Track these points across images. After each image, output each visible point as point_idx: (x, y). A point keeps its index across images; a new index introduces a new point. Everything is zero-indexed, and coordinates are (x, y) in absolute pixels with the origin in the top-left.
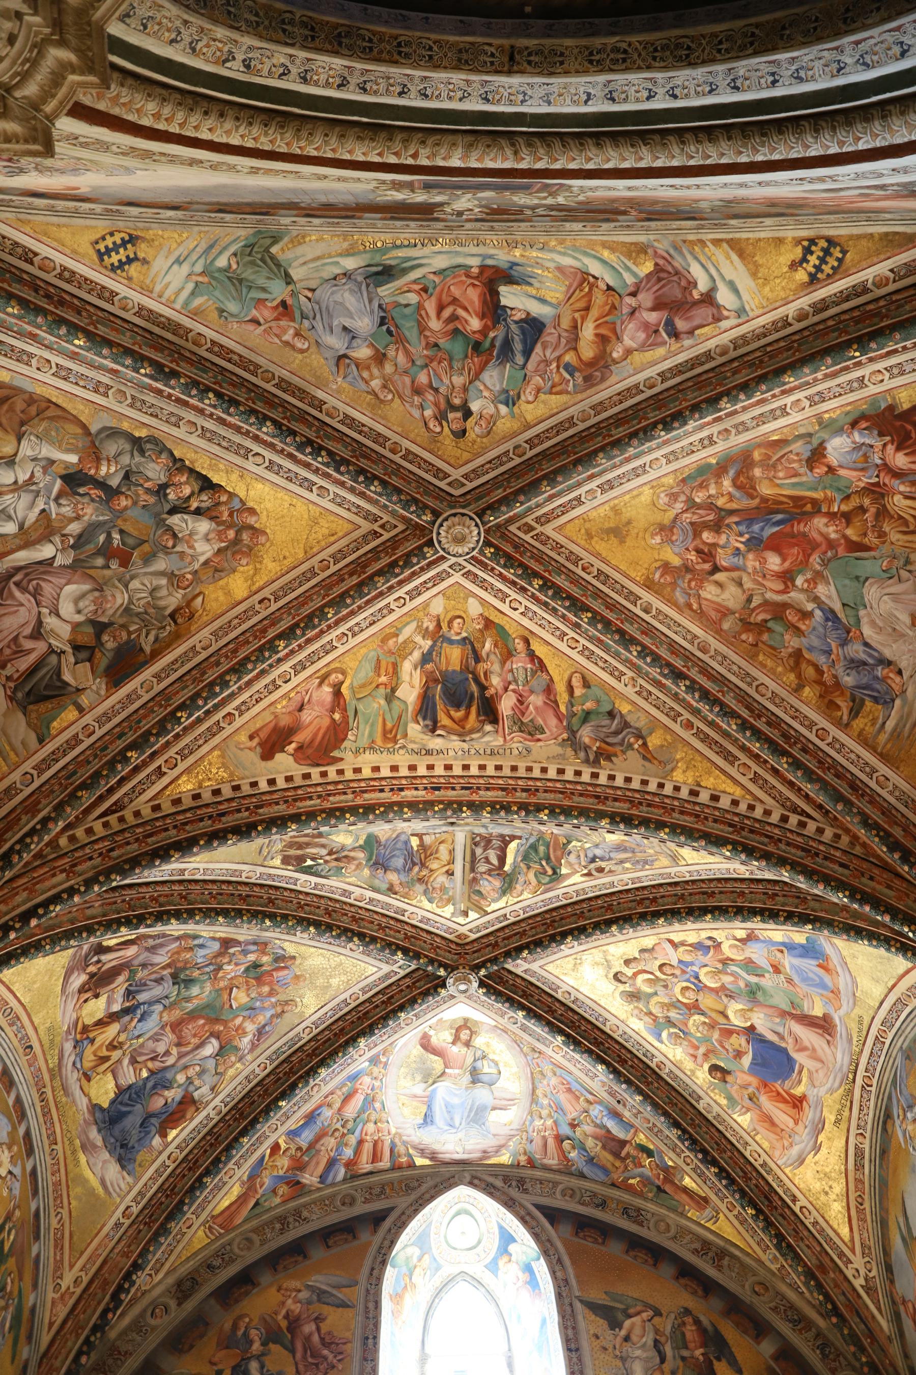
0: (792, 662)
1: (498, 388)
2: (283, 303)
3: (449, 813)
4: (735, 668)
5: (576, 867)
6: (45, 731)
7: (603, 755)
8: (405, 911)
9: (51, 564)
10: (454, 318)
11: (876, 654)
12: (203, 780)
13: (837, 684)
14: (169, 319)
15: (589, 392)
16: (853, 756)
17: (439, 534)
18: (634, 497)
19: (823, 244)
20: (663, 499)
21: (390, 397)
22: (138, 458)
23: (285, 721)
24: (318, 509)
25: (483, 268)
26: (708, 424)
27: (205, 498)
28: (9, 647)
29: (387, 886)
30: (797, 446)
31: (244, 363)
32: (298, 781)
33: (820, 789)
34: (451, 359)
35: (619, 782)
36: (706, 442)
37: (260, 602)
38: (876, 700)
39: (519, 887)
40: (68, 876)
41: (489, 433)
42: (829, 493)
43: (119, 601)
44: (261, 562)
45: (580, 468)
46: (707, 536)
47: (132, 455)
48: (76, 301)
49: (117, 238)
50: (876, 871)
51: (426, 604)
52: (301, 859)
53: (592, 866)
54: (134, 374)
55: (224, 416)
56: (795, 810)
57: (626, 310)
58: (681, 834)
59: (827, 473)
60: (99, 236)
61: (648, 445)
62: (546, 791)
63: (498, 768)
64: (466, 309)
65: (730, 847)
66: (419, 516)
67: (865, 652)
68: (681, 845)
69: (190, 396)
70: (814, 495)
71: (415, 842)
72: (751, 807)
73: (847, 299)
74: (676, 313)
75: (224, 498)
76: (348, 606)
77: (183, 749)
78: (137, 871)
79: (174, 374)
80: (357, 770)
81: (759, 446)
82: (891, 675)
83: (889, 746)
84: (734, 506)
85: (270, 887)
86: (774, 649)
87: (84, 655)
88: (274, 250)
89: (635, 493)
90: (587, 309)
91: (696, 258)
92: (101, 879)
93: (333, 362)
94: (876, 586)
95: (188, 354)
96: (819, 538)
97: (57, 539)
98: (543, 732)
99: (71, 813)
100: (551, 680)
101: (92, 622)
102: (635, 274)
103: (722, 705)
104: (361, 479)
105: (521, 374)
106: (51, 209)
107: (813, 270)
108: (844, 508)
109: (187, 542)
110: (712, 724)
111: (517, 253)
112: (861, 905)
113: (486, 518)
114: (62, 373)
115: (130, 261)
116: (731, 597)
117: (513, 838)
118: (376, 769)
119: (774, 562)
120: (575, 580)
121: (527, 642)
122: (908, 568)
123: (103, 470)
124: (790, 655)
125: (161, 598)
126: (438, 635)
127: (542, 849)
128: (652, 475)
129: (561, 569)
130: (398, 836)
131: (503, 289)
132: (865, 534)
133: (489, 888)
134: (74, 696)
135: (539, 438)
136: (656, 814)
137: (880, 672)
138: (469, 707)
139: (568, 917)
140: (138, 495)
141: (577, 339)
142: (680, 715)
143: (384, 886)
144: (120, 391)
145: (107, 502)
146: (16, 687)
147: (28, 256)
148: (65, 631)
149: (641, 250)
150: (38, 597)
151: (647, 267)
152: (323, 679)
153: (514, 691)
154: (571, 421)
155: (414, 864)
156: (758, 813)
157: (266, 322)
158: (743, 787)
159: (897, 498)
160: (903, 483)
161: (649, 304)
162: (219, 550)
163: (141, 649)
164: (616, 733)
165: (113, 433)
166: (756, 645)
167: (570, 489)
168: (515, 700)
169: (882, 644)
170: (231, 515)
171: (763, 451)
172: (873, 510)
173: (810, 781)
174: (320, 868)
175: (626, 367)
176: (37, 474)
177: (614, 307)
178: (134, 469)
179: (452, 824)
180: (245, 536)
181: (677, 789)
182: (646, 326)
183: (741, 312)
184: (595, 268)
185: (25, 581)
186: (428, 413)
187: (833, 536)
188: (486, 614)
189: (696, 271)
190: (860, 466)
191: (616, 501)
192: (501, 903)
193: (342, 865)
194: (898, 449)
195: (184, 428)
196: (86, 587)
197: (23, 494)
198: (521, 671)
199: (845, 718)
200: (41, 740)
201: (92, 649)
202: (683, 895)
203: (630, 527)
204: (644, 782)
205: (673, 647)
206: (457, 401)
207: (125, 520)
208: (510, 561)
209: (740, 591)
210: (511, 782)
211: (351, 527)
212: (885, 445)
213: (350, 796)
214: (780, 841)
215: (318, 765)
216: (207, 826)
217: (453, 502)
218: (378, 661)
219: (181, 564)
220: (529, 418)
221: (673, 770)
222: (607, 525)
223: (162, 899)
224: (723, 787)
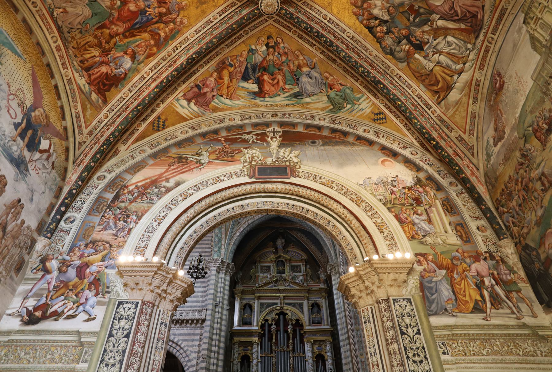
2: (331, 89)
9: (441, 17)
10: (273, 80)
15: (223, 58)
20: (185, 21)
21: (296, 52)
22: (393, 48)
25: (264, 97)
27: (372, 24)
30: (141, 58)
31: (347, 72)
34: (274, 65)
36: (175, 49)
41: (258, 38)
46: (164, 10)
49: (379, 122)
59: (127, 51)
64: (269, 83)
70: (126, 40)
73: (147, 116)
75: (365, 22)
81: (154, 54)
84: (156, 25)
88: (332, 107)
90: (228, 87)
94: (87, 14)
97: (434, 26)
102: (215, 102)
105: (248, 61)
108: (114, 40)
109: (384, 6)
113: (258, 11)
115: (377, 114)
122: (79, 30)
123: (407, 47)
131: (257, 90)
132: (102, 33)
135: (239, 38)
140: (398, 33)
141: (230, 76)
144: (392, 74)
154: (228, 46)
159: (98, 54)
160: (99, 61)
161: (208, 94)
165: (400, 60)
170: (364, 14)
171: (153, 52)
172: (104, 44)
176: (431, 55)
177: (219, 90)
178: (396, 44)
182: (207, 86)
184: (228, 101)
185: (454, 15)
186: (282, 45)
189: (195, 108)
190: (116, 60)
194: (107, 73)
195: (374, 54)
206: (271, 50)
207: (406, 24)
212: (112, 72)
220: (243, 45)
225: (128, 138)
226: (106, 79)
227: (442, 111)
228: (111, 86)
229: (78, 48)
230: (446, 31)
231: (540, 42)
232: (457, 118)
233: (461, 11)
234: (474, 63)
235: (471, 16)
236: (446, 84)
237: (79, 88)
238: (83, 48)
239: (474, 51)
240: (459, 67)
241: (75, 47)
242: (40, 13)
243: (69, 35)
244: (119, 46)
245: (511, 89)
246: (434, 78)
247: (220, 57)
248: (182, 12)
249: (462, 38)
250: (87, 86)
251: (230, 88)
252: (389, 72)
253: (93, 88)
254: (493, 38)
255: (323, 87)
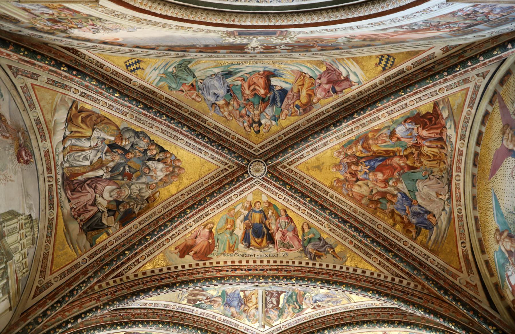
0: (390, 215)
1: (271, 115)
2: (192, 85)
3: (255, 280)
4: (368, 218)
5: (309, 305)
6: (93, 242)
7: (317, 256)
8: (239, 325)
9: (102, 178)
10: (254, 89)
11: (424, 209)
12: (156, 265)
13: (410, 223)
14: (150, 89)
15: (305, 115)
16: (419, 252)
17: (250, 168)
18: (324, 154)
19: (386, 57)
20: (336, 154)
21: (231, 118)
22: (137, 139)
23: (190, 242)
24: (204, 160)
25: (264, 71)
26: (350, 124)
28: (82, 208)
29: (231, 314)
30: (385, 131)
31: (178, 106)
32: (194, 267)
33: (407, 265)
34: (254, 105)
35: (324, 266)
36: (350, 131)
37: (181, 195)
38: (426, 228)
39: (285, 314)
40: (96, 302)
41: (268, 131)
42: (399, 148)
43: (127, 193)
44: (182, 180)
45: (303, 143)
46: (353, 167)
47: (135, 138)
48: (117, 82)
49: (133, 61)
50: (434, 300)
51: (246, 197)
52: (195, 301)
53: (315, 304)
54: (137, 108)
55: (169, 124)
56: (397, 275)
57: (317, 85)
58: (350, 287)
60: (127, 60)
61: (328, 133)
62: (294, 271)
63: (275, 262)
64: (259, 86)
65: (371, 292)
66: (242, 162)
67: (419, 209)
68: (351, 293)
69: (157, 116)
71: (242, 294)
72: (379, 275)
73: (397, 75)
74: (335, 85)
75: (169, 155)
76: (215, 197)
77: (148, 252)
78: (125, 301)
79: (151, 108)
80: (218, 263)
81: (371, 132)
82: (431, 217)
83: (433, 246)
84: (363, 155)
85: (182, 313)
86: (383, 210)
87: (111, 213)
88: (189, 66)
89: (325, 152)
90: (303, 85)
91: (341, 65)
92: (110, 303)
93: (210, 106)
94: (421, 183)
95: (157, 102)
96: (397, 166)
97: (104, 168)
98: (293, 247)
99: (101, 275)
100: (295, 226)
101: (116, 201)
102: (319, 72)
103: (364, 233)
104: (220, 148)
106: (111, 50)
107: (384, 66)
108: (405, 153)
109: (154, 172)
110: (360, 241)
111: (277, 66)
112: (429, 315)
113: (268, 163)
114: (111, 107)
115: (137, 69)
116: (364, 190)
117: (282, 292)
118: (226, 262)
119: (380, 176)
120: (303, 186)
121: (285, 211)
122: (433, 174)
123: (124, 143)
124: (390, 212)
125: (143, 193)
126: (250, 209)
127: (294, 297)
128: (331, 145)
129: (297, 182)
130: (235, 292)
131: (272, 79)
132: (414, 163)
133: (273, 315)
134: (106, 229)
135: (287, 133)
136: (340, 279)
137: (426, 216)
138: (263, 238)
139: (307, 328)
140: (136, 153)
141: (300, 96)
142: (347, 238)
143: (230, 314)
144: (131, 114)
145: (125, 155)
146: (84, 225)
147: (101, 66)
148: (105, 204)
149: (321, 63)
150: (96, 190)
151: (324, 69)
152: (205, 226)
153: (281, 231)
154: (299, 127)
155: (242, 304)
156: (382, 277)
157: (186, 91)
158: (375, 267)
159: (425, 148)
160: (427, 142)
161: (325, 82)
162: (166, 175)
163: (134, 212)
164: (322, 247)
165: (128, 130)
166: (376, 209)
167: (300, 151)
168: (281, 235)
169: (426, 205)
170: (171, 162)
171: (372, 133)
172: (416, 153)
173: (402, 262)
174: (203, 305)
175: (318, 105)
176: (99, 144)
177: (313, 83)
179: (257, 286)
180: (176, 170)
181: (348, 269)
183: (359, 83)
184: (305, 70)
186: (246, 124)
187: (402, 164)
188: (269, 201)
189: (341, 69)
190: (409, 137)
191: (318, 156)
192: (278, 322)
193: (212, 304)
194: (423, 129)
195: (154, 129)
196: (114, 187)
197: (93, 151)
198: (283, 223)
199: (414, 236)
200: (92, 246)
201: (115, 211)
202: (354, 316)
203: (324, 165)
204: (335, 267)
205: (343, 211)
206: (256, 120)
208: (277, 179)
209: (367, 188)
210: (280, 267)
211: (217, 167)
212: (418, 128)
213: (215, 273)
214: (392, 288)
215: (202, 260)
216: (156, 283)
217: (255, 157)
218: (227, 219)
219: (151, 180)
220: (284, 125)
221: (346, 261)
222: (315, 165)
223: (136, 316)
224: (367, 267)
225: (426, 59)
226: (426, 124)
227: (67, 96)
228: (424, 116)
229: (440, 160)
230: (93, 167)
231: (7, 221)
232: (48, 96)
233: (86, 189)
234: (56, 153)
235: (76, 190)
236: (74, 123)
237: (456, 128)
238: (436, 158)
239: (60, 163)
240: (68, 144)
241: (442, 163)
242: (459, 203)
243: (443, 175)
244: (402, 146)
245: (10, 166)
246: (88, 123)
247: (308, 117)
248: (338, 162)
249: (76, 168)
250: (448, 127)
251: (301, 83)
252: (135, 115)
253: (443, 122)
254: (49, 181)
255: (201, 85)
